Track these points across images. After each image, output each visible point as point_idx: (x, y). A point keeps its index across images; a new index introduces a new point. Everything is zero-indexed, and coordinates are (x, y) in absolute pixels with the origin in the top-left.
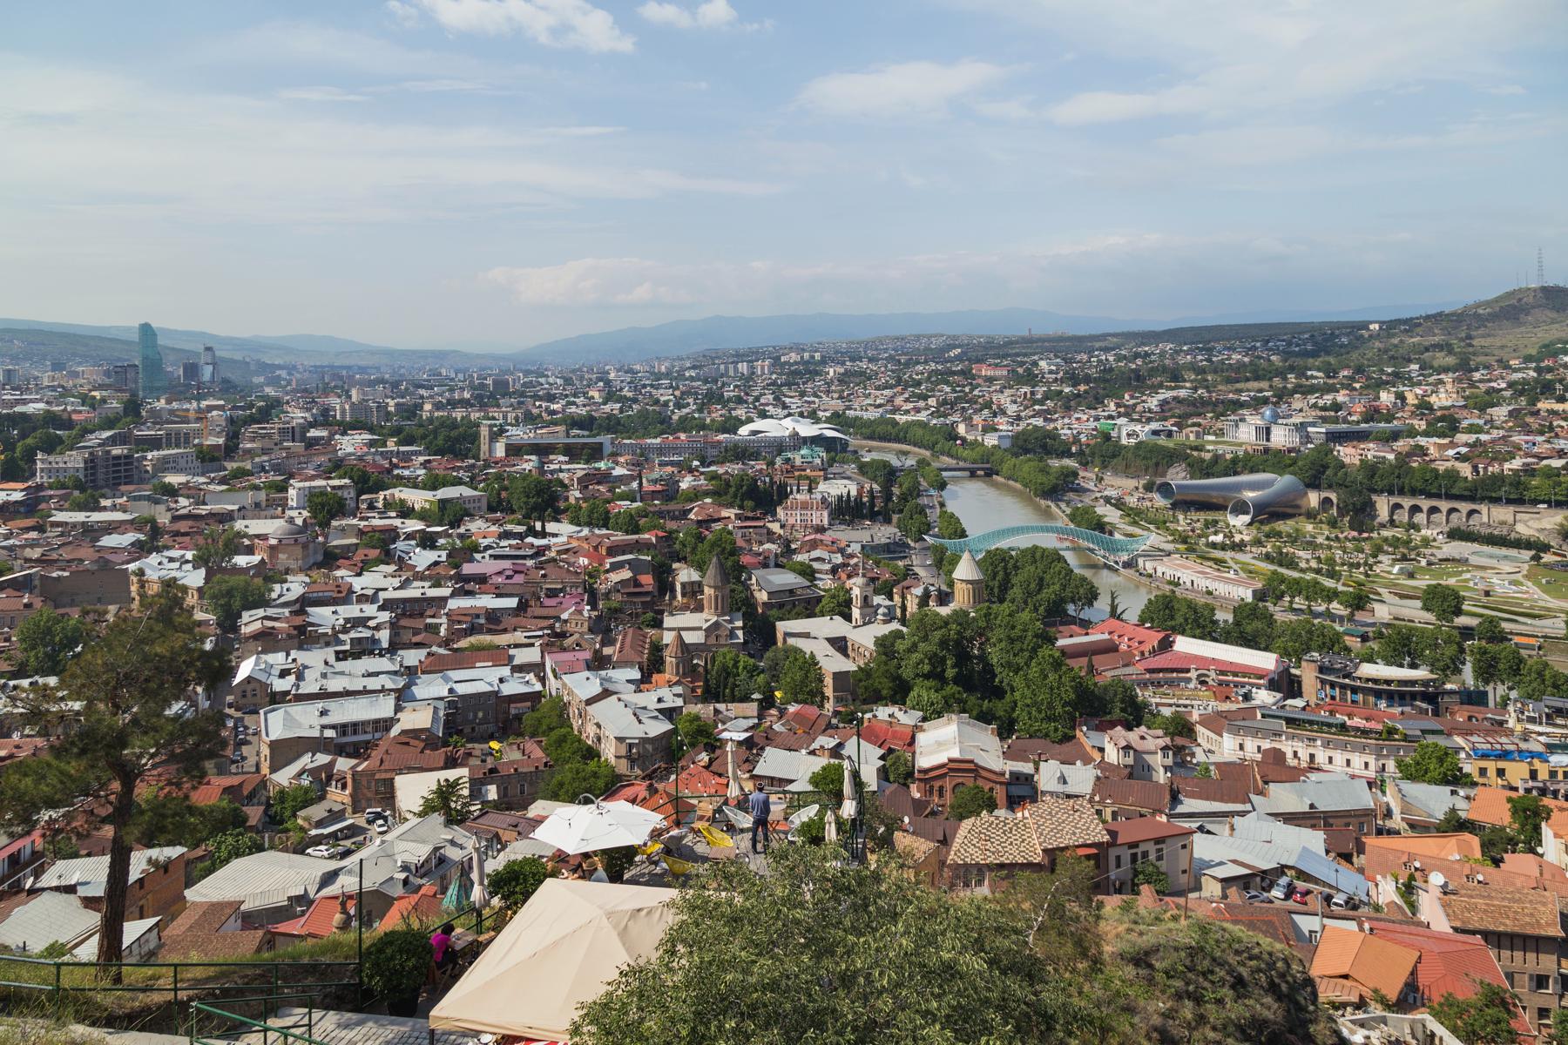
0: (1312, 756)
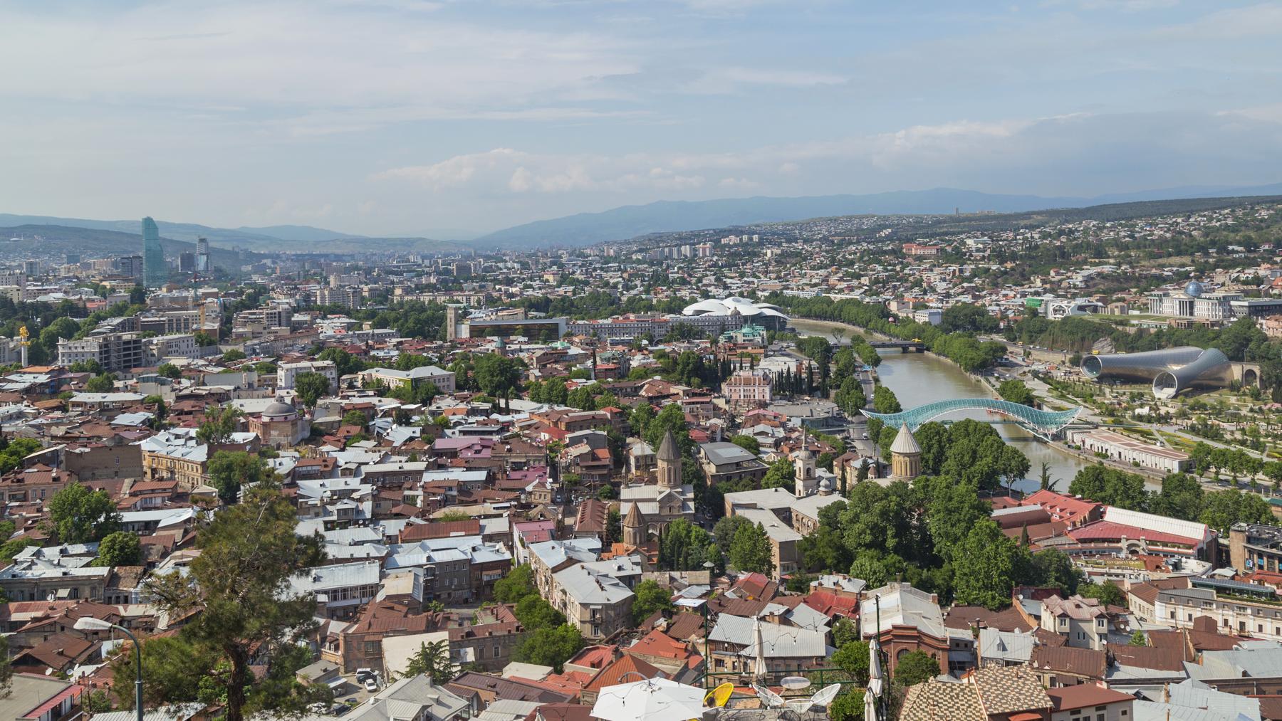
0: (1242, 624)
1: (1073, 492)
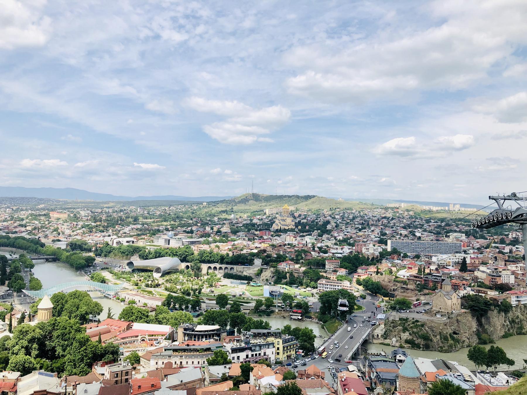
0: (181, 362)
1: (120, 319)
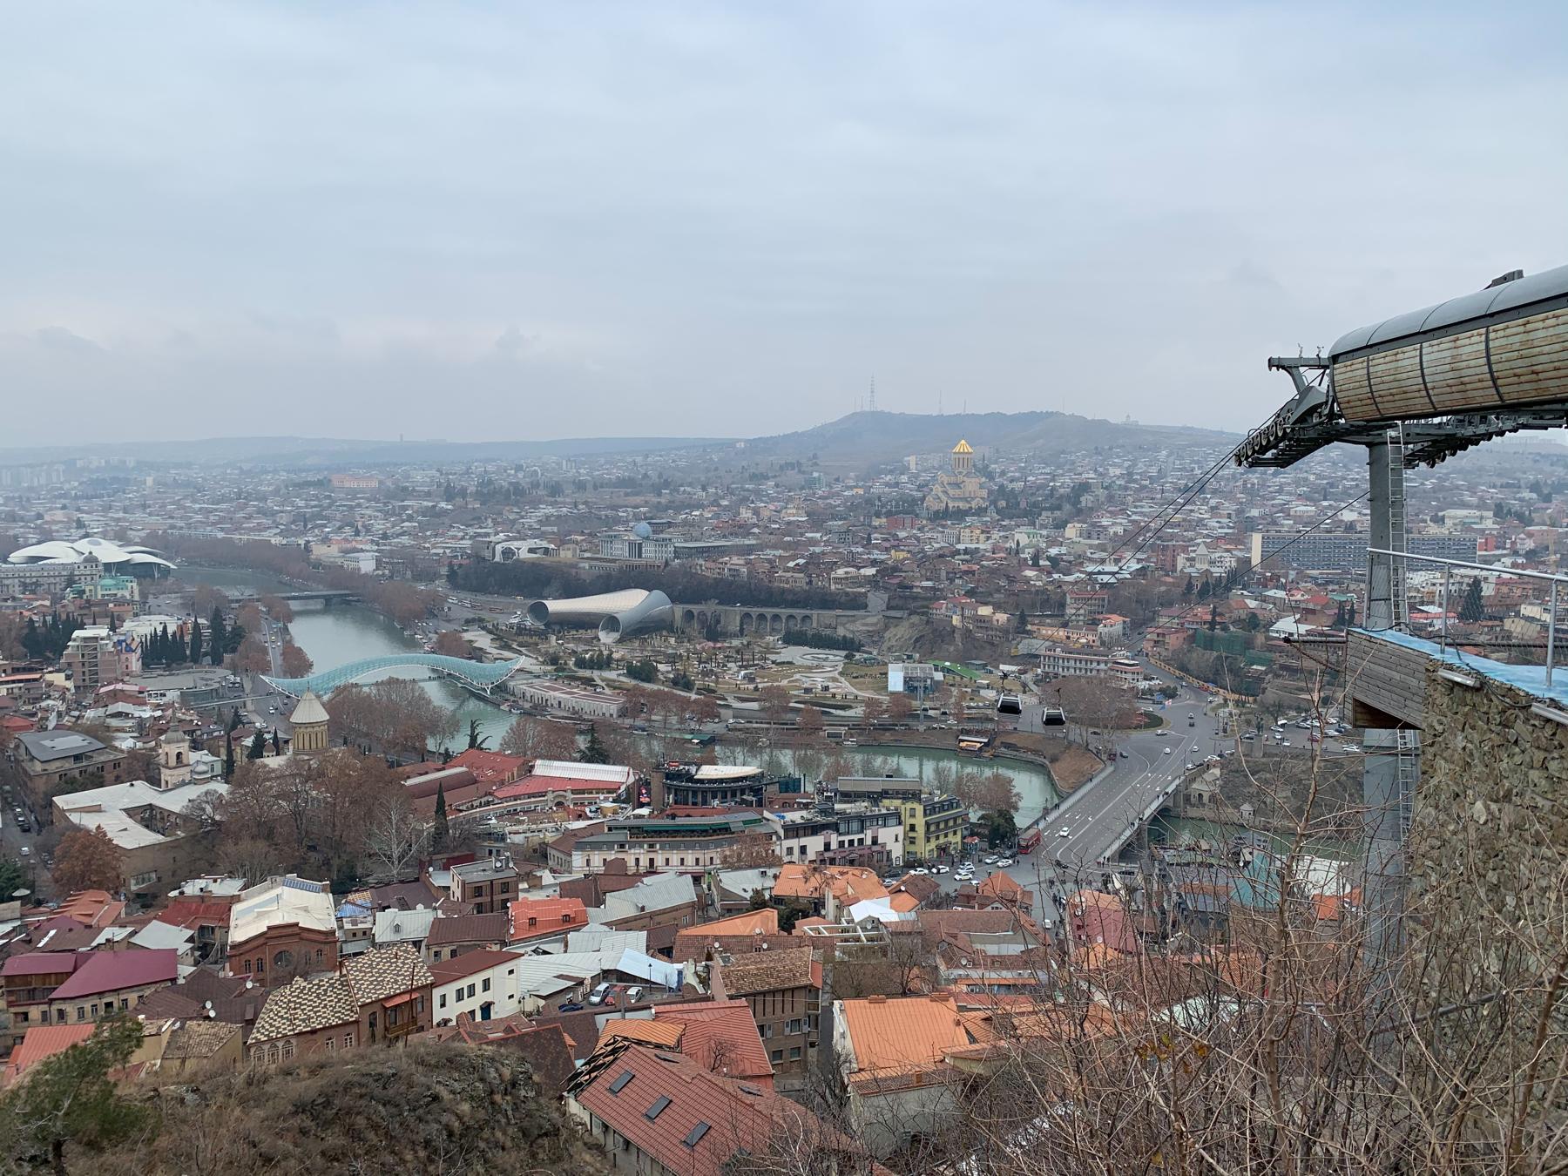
0: (652, 861)
